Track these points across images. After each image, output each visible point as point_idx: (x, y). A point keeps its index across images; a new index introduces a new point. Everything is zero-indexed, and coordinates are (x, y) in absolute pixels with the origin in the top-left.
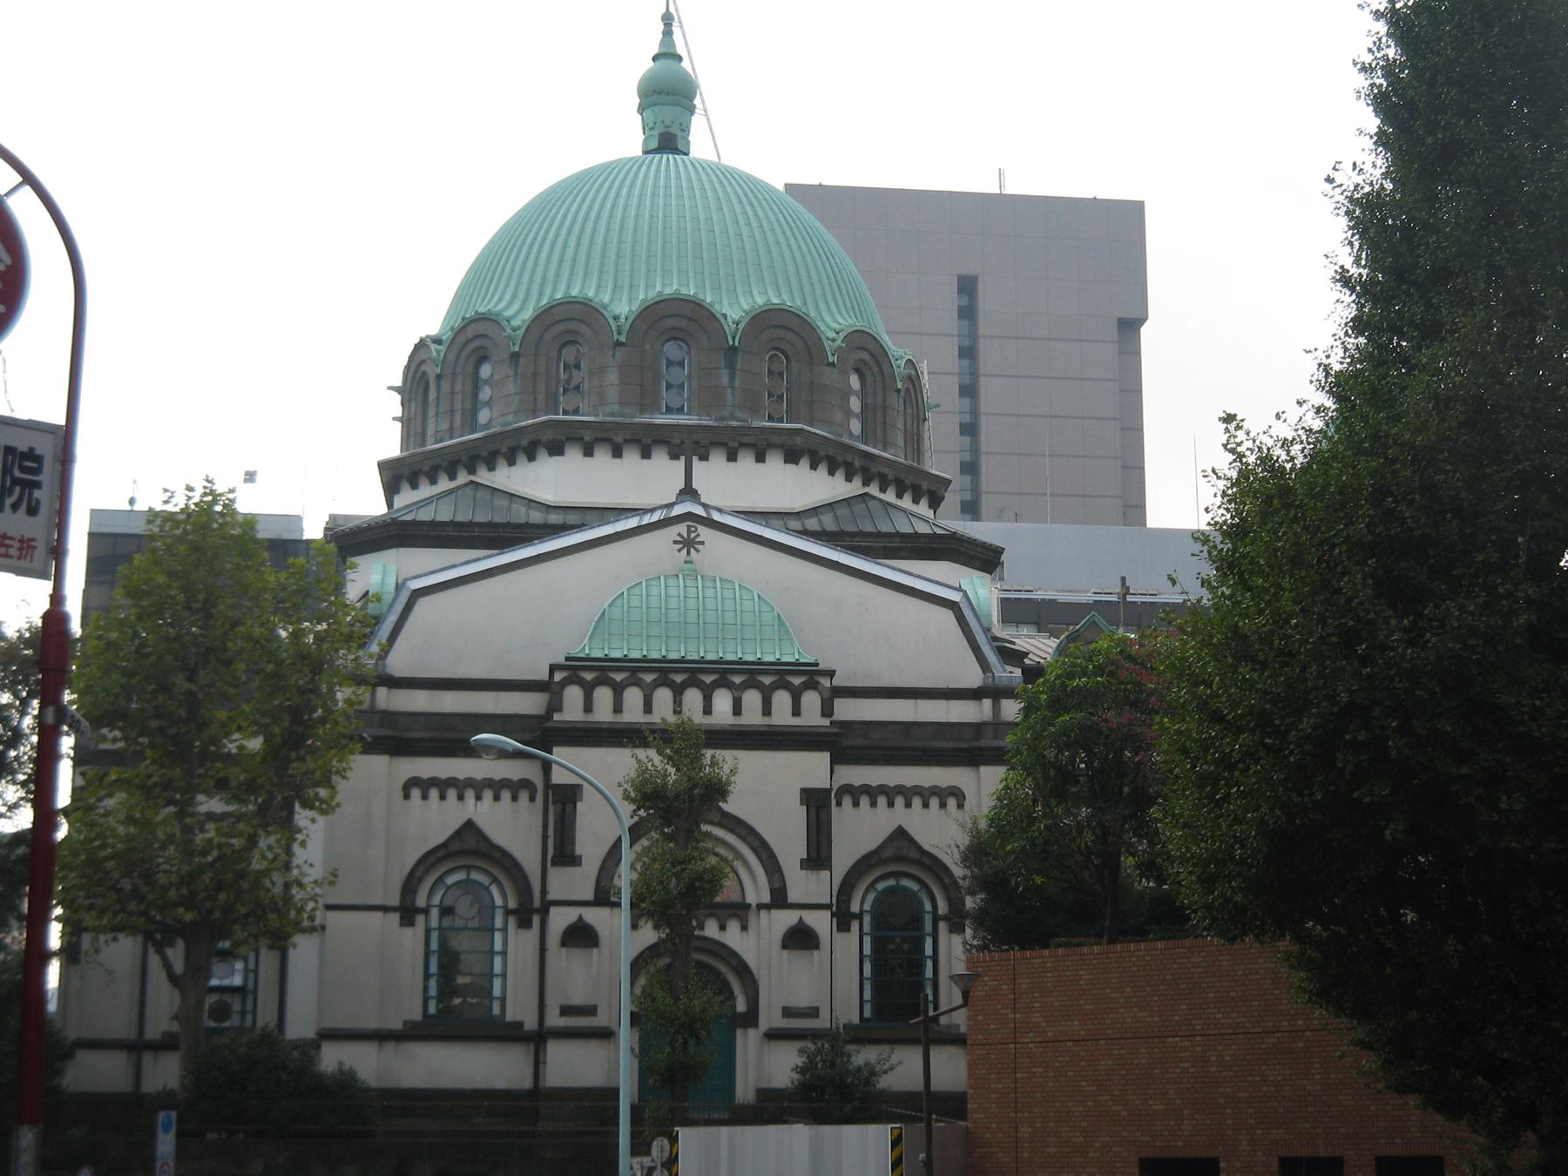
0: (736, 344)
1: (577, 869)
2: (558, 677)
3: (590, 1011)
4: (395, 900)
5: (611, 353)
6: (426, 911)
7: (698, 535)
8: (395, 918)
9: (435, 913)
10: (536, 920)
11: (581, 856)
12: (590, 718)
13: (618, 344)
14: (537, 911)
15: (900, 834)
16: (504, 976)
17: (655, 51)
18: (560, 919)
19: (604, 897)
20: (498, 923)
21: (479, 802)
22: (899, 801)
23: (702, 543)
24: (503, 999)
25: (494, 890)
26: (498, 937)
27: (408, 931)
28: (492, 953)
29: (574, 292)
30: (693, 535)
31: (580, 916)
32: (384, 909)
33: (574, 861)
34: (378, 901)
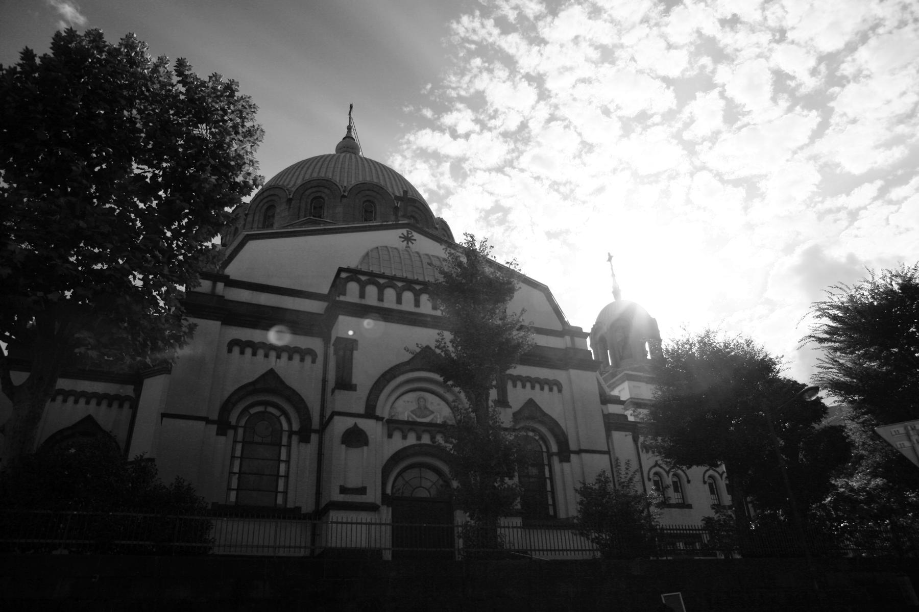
0: (399, 206)
1: (355, 392)
2: (343, 275)
3: (362, 491)
4: (215, 416)
5: (339, 200)
6: (235, 428)
7: (413, 236)
8: (215, 427)
9: (240, 431)
10: (314, 437)
11: (356, 385)
12: (363, 302)
13: (343, 196)
14: (315, 431)
15: (531, 402)
16: (287, 476)
17: (344, 136)
18: (341, 425)
19: (370, 413)
20: (285, 441)
21: (278, 360)
22: (528, 385)
23: (415, 240)
24: (285, 493)
25: (283, 419)
26: (284, 451)
27: (222, 439)
28: (279, 461)
29: (322, 175)
30: (410, 236)
31: (356, 423)
32: (207, 420)
33: (351, 387)
34: (203, 414)
